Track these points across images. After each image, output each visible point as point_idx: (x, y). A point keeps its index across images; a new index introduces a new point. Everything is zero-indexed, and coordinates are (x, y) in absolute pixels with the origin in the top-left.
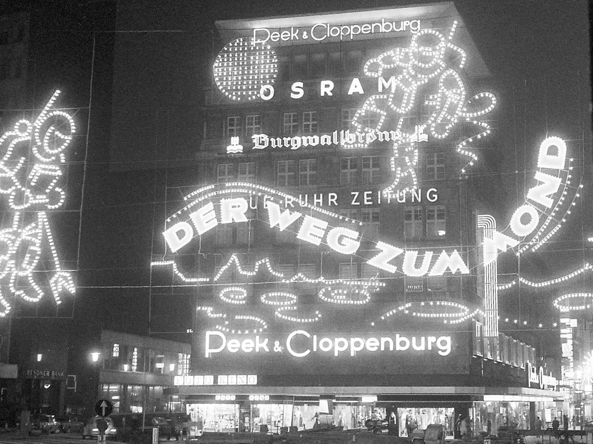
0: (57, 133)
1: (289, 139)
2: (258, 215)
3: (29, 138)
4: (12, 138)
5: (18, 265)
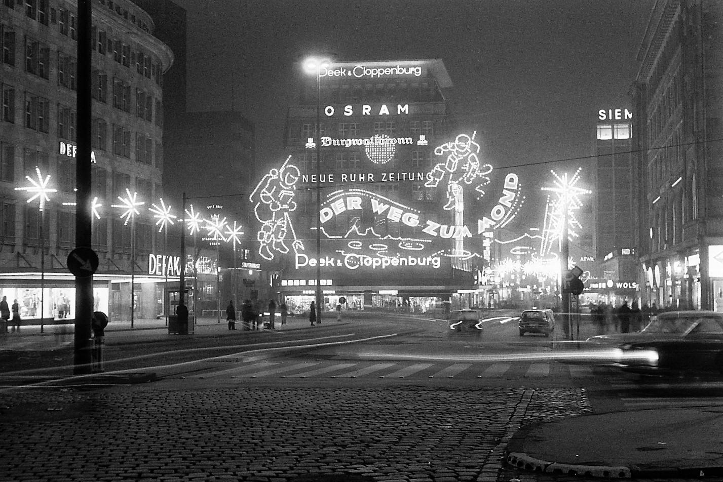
0: (291, 176)
1: (344, 140)
2: (366, 203)
3: (277, 178)
4: (268, 178)
5: (277, 238)
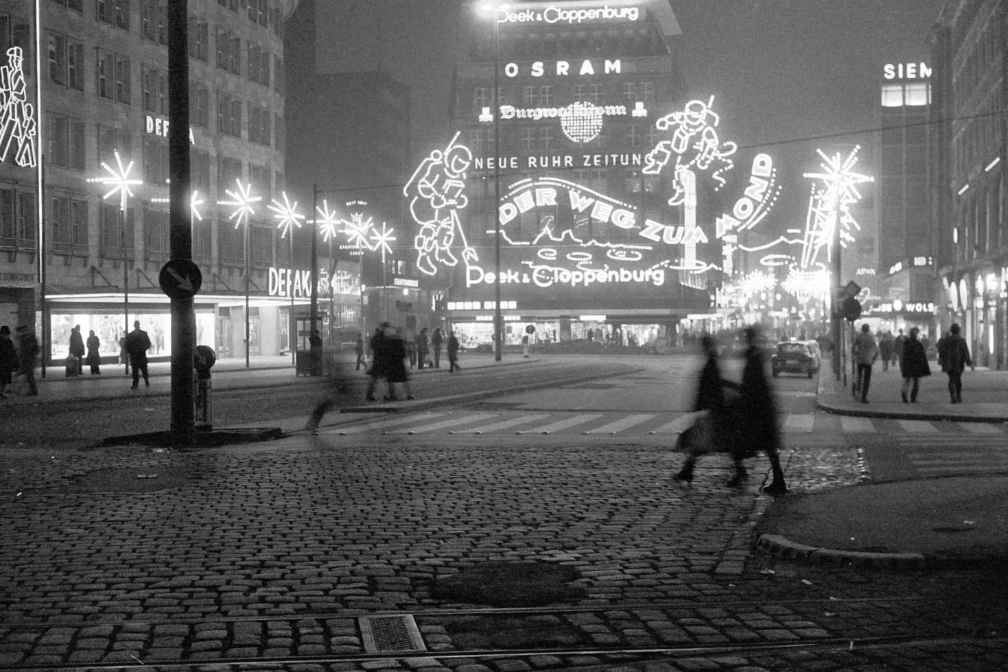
3: (441, 162)
4: (429, 162)
5: (440, 244)
